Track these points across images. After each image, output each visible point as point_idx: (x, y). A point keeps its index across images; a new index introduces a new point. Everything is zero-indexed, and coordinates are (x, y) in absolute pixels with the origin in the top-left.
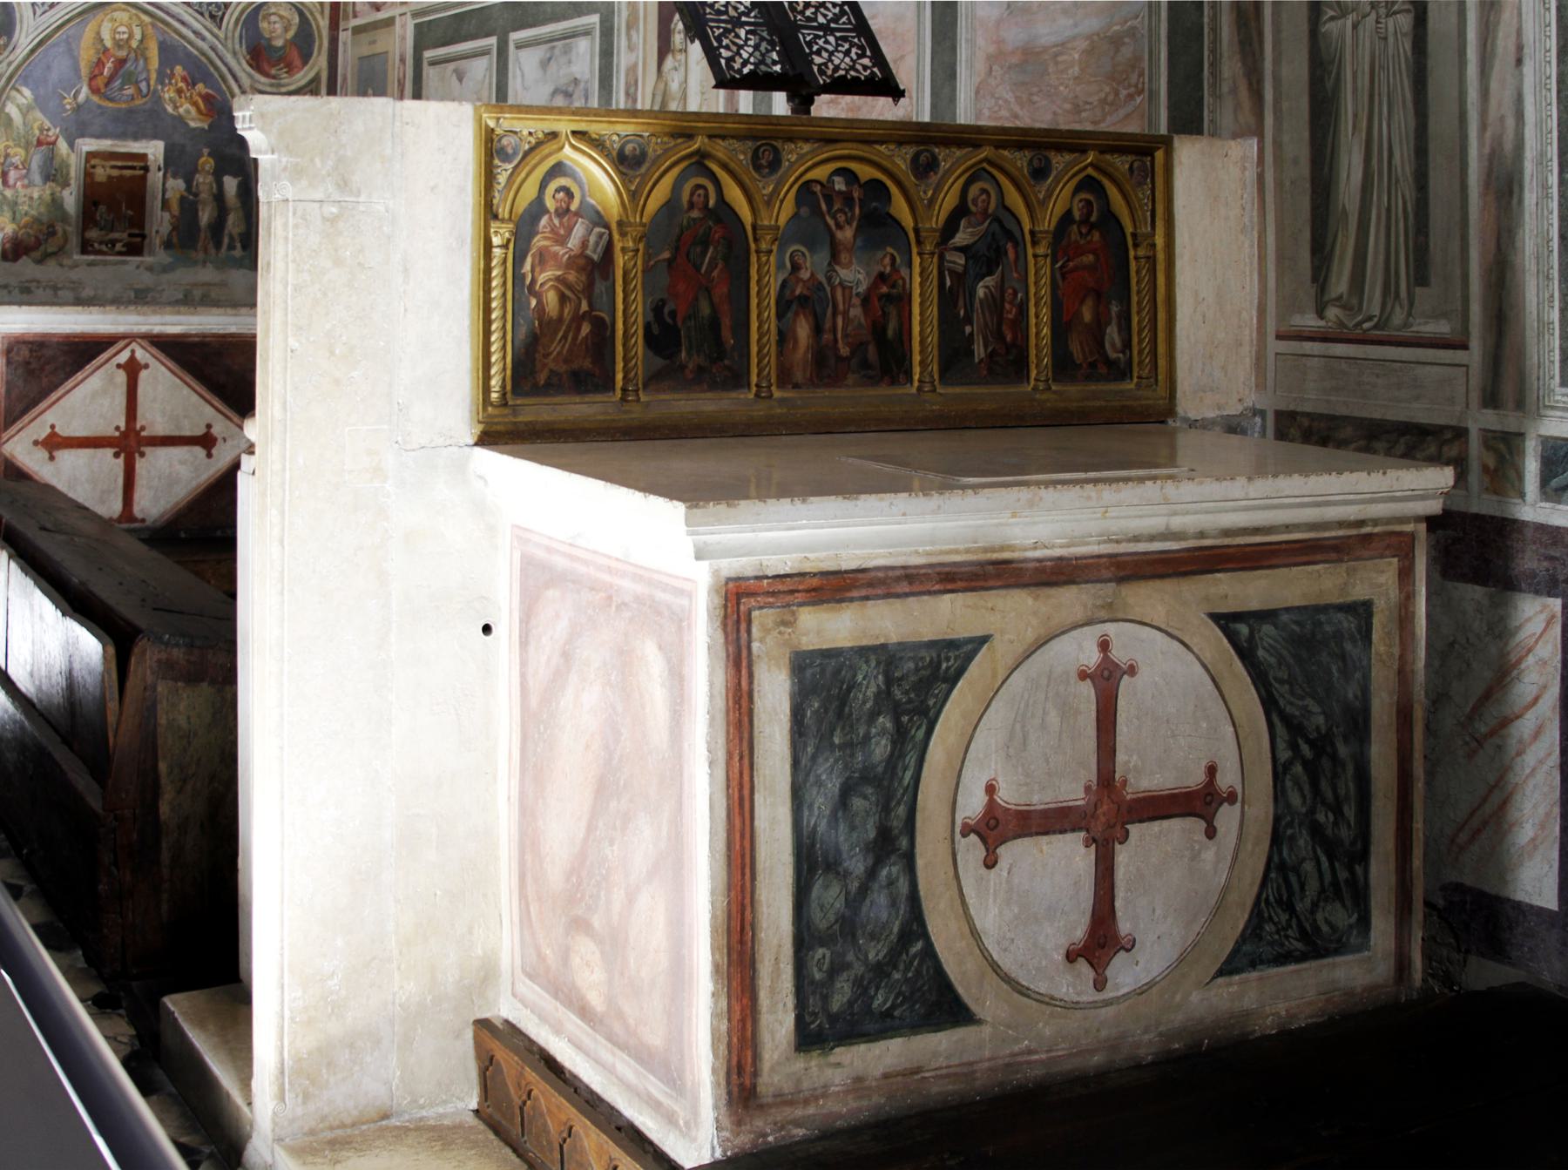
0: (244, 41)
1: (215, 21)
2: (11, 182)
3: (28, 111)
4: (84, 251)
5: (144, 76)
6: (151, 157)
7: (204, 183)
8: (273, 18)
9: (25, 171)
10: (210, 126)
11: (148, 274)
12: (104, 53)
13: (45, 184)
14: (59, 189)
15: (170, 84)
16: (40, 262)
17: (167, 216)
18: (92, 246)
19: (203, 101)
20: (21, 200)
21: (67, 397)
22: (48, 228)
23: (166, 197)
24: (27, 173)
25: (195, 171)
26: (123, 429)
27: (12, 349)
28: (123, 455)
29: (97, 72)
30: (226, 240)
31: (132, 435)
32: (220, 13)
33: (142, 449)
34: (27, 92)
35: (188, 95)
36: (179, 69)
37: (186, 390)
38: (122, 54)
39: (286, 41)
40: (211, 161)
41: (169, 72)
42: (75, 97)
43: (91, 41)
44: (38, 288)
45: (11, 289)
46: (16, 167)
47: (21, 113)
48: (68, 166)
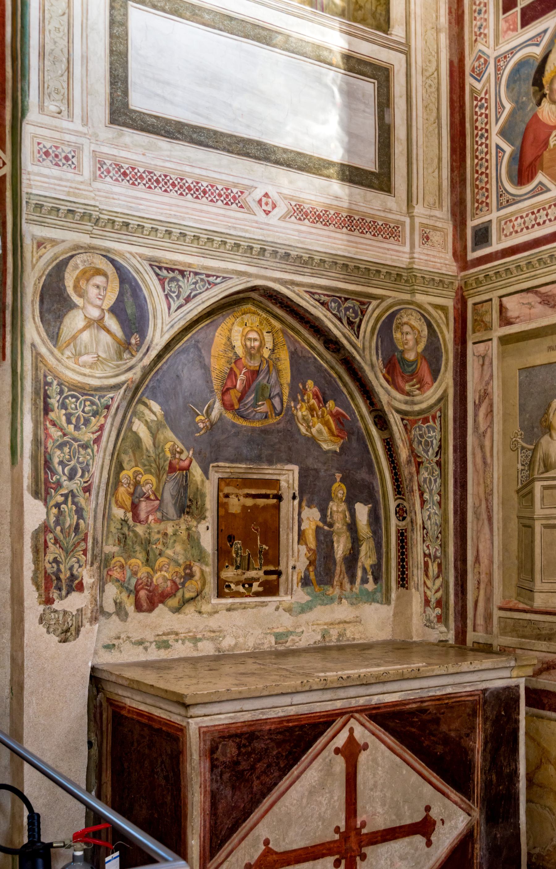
0: (380, 352)
1: (353, 329)
2: (143, 516)
3: (158, 430)
4: (220, 595)
5: (276, 391)
6: (283, 484)
7: (338, 512)
8: (406, 328)
9: (158, 502)
10: (341, 448)
11: (287, 615)
12: (235, 363)
13: (180, 517)
14: (195, 523)
15: (303, 400)
16: (177, 610)
17: (303, 549)
18: (229, 587)
19: (334, 421)
20: (155, 537)
21: (282, 799)
22: (185, 569)
23: (302, 528)
24: (160, 505)
25: (329, 498)
26: (343, 829)
27: (217, 748)
28: (343, 862)
29: (229, 385)
30: (359, 573)
31: (353, 834)
32: (357, 320)
33: (364, 850)
34: (156, 407)
35: (320, 413)
36: (310, 384)
37: (406, 769)
38: (254, 364)
40: (343, 486)
41: (301, 387)
42: (208, 413)
43: (222, 347)
44: (177, 641)
45: (147, 644)
46: (148, 498)
47: (151, 432)
48: (203, 496)
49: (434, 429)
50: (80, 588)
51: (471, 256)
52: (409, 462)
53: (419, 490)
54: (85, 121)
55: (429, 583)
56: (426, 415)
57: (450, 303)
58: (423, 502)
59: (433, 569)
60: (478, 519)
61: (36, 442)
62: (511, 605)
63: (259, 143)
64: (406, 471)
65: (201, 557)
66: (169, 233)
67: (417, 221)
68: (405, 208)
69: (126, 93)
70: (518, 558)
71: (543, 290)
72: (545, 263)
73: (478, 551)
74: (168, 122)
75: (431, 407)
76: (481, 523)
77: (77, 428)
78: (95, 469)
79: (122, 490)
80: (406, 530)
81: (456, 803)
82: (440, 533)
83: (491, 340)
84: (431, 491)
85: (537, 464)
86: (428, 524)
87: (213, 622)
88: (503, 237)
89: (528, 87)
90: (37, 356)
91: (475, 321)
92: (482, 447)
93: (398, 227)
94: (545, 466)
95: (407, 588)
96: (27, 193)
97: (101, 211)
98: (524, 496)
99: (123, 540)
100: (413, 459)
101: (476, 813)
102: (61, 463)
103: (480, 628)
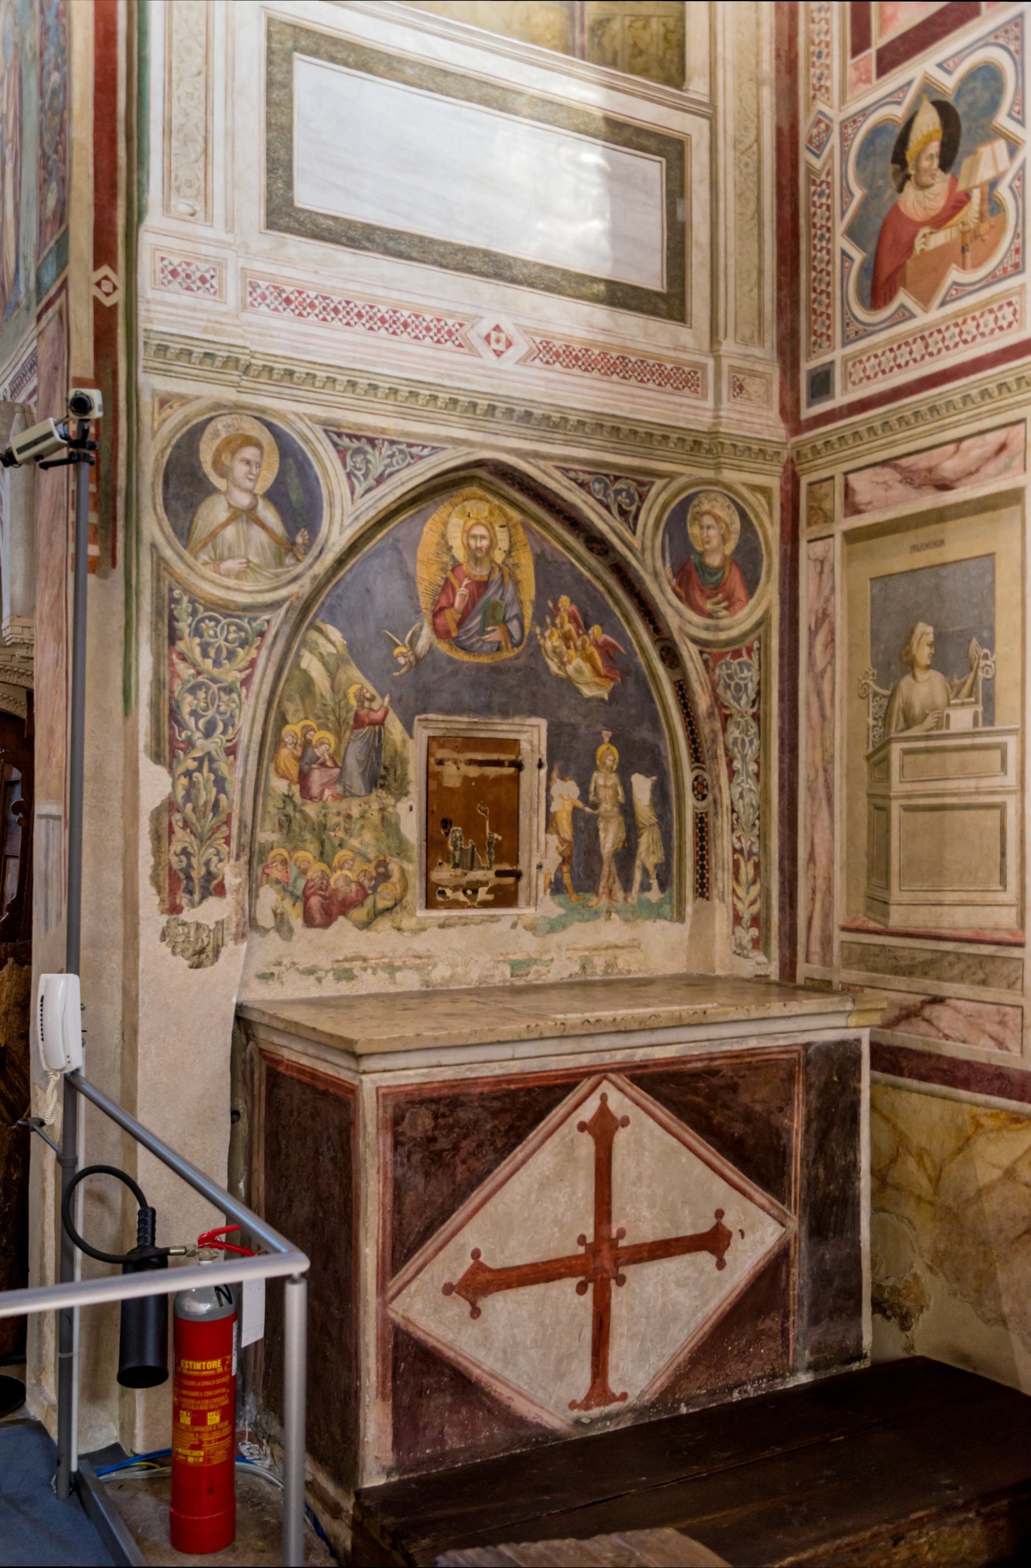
0: (667, 555)
1: (627, 521)
2: (315, 790)
3: (338, 667)
4: (430, 903)
5: (513, 611)
6: (525, 746)
7: (605, 786)
8: (707, 520)
9: (337, 771)
10: (612, 694)
11: (529, 934)
12: (453, 570)
13: (370, 792)
14: (392, 801)
15: (554, 625)
16: (365, 925)
17: (554, 840)
18: (442, 893)
19: (600, 655)
20: (333, 820)
21: (499, 1193)
22: (377, 867)
23: (552, 809)
24: (341, 775)
25: (593, 767)
26: (590, 1240)
27: (403, 1118)
28: (591, 1286)
29: (444, 602)
30: (638, 876)
31: (605, 1247)
32: (633, 508)
33: (623, 1270)
34: (335, 634)
35: (579, 643)
36: (564, 601)
37: (686, 1156)
38: (481, 572)
39: (725, 557)
40: (614, 750)
41: (551, 605)
42: (412, 644)
43: (433, 549)
44: (365, 969)
45: (321, 974)
46: (323, 765)
47: (328, 670)
48: (404, 762)
49: (749, 667)
50: (220, 891)
51: (807, 413)
52: (711, 715)
53: (727, 755)
54: (230, 226)
55: (741, 892)
56: (736, 647)
57: (774, 483)
58: (732, 773)
59: (747, 871)
60: (813, 799)
61: (158, 683)
62: (858, 924)
63: (486, 254)
64: (705, 729)
65: (402, 850)
66: (353, 384)
67: (725, 363)
68: (706, 344)
69: (289, 185)
70: (868, 854)
71: (904, 462)
72: (907, 424)
73: (812, 844)
74: (351, 224)
75: (745, 635)
76: (817, 804)
77: (217, 663)
78: (243, 722)
79: (284, 752)
80: (706, 814)
81: (762, 1207)
82: (758, 818)
83: (832, 536)
84: (744, 758)
85: (895, 718)
86: (739, 805)
87: (419, 944)
88: (850, 386)
89: (885, 165)
90: (160, 563)
91: (810, 508)
92: (819, 693)
93: (696, 373)
94: (906, 720)
95: (708, 899)
96: (146, 330)
97: (253, 354)
98: (877, 764)
99: (286, 824)
100: (716, 711)
101: (794, 1223)
102: (194, 713)
103: (815, 958)
